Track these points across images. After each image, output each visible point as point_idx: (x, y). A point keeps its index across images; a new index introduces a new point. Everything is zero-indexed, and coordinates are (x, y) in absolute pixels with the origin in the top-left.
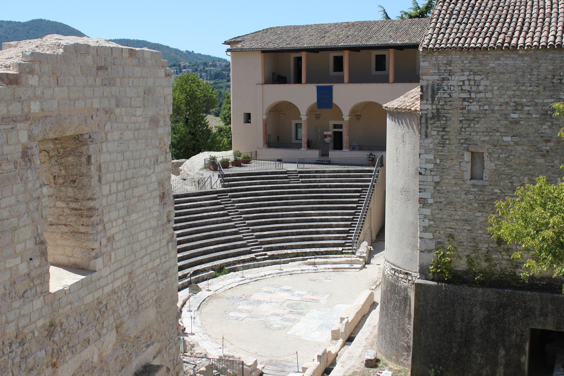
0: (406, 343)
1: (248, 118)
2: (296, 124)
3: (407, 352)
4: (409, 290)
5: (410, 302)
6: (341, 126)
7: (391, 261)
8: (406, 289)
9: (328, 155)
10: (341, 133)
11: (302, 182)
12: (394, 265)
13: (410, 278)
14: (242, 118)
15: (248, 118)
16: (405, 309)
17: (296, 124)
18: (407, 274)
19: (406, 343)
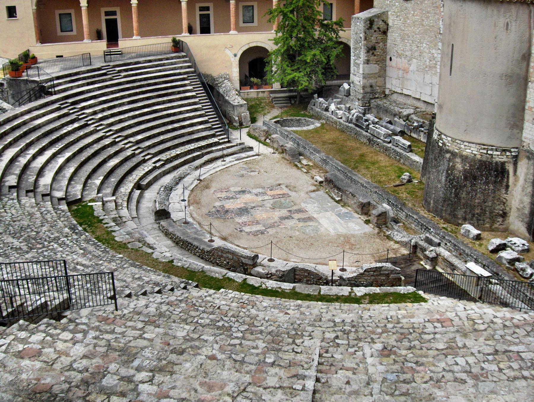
0: (502, 210)
1: (11, 12)
2: (70, 14)
3: (503, 217)
4: (506, 164)
5: (508, 174)
6: (114, 13)
7: (479, 142)
8: (503, 164)
9: (117, 45)
10: (115, 21)
11: (125, 77)
12: (484, 145)
13: (508, 154)
14: (5, 13)
15: (11, 12)
16: (501, 182)
17: (70, 14)
18: (504, 151)
19: (502, 210)
